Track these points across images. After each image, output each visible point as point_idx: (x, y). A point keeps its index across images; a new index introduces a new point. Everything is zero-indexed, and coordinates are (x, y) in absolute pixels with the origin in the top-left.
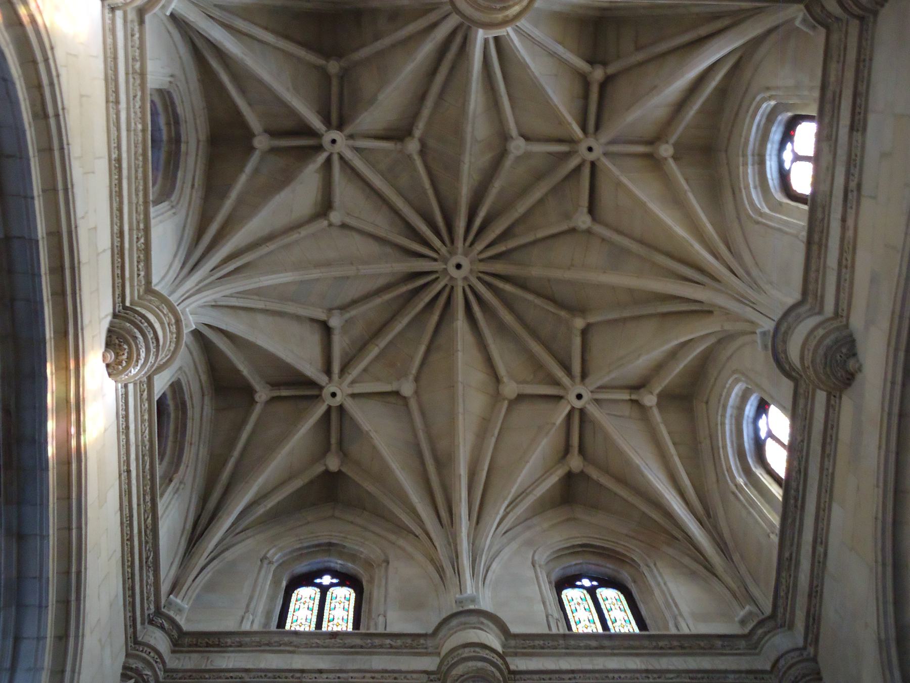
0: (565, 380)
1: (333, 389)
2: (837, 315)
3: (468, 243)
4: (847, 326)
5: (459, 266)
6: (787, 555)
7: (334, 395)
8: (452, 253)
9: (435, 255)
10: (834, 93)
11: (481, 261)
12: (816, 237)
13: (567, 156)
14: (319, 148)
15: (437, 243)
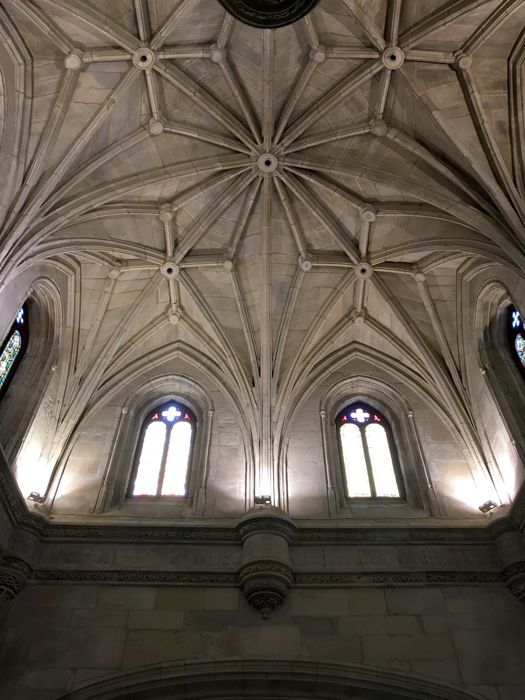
0: (180, 257)
1: (149, 57)
2: (295, 575)
3: (287, 168)
4: (289, 588)
5: (268, 163)
6: (101, 533)
7: (144, 59)
8: (278, 157)
9: (276, 141)
10: (443, 539)
11: (272, 178)
12: (342, 535)
13: (356, 246)
14: (386, 37)
15: (287, 142)
